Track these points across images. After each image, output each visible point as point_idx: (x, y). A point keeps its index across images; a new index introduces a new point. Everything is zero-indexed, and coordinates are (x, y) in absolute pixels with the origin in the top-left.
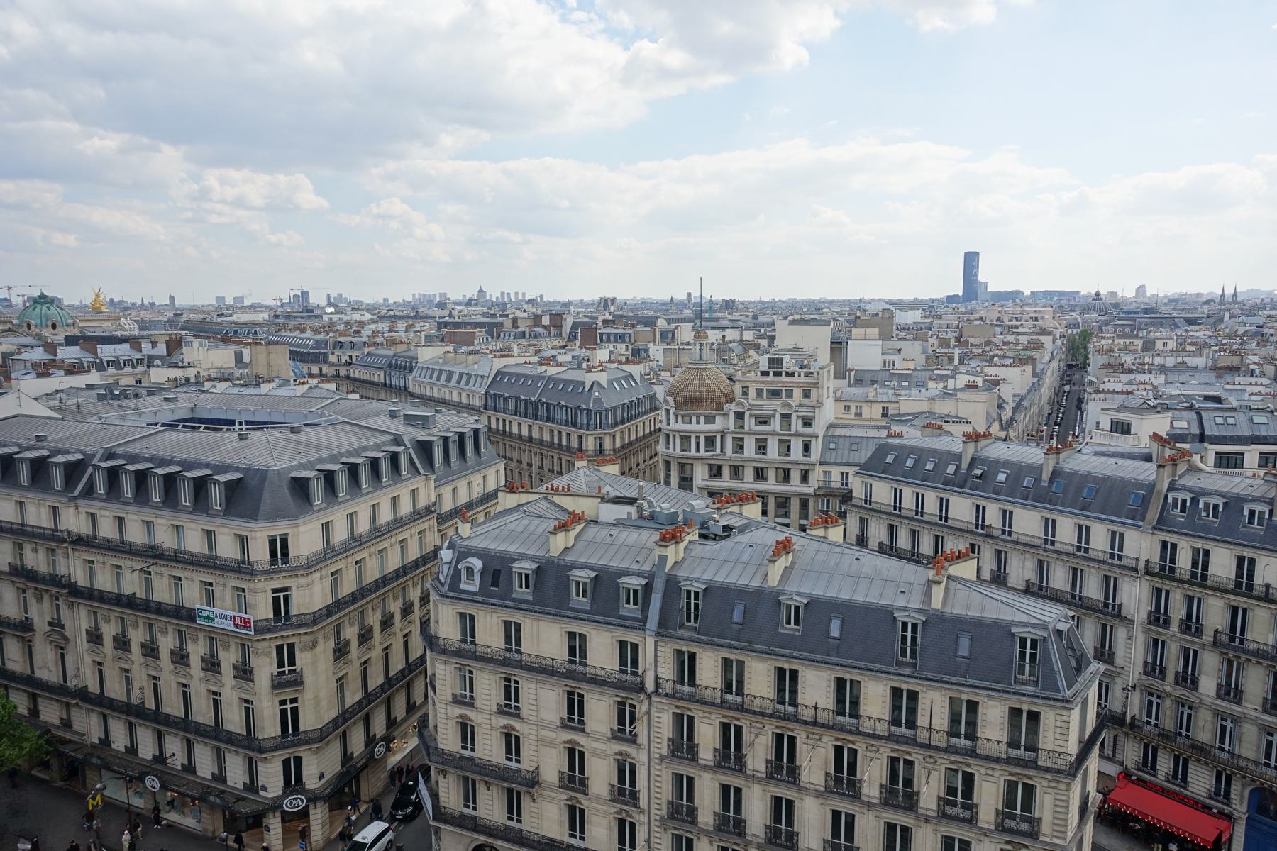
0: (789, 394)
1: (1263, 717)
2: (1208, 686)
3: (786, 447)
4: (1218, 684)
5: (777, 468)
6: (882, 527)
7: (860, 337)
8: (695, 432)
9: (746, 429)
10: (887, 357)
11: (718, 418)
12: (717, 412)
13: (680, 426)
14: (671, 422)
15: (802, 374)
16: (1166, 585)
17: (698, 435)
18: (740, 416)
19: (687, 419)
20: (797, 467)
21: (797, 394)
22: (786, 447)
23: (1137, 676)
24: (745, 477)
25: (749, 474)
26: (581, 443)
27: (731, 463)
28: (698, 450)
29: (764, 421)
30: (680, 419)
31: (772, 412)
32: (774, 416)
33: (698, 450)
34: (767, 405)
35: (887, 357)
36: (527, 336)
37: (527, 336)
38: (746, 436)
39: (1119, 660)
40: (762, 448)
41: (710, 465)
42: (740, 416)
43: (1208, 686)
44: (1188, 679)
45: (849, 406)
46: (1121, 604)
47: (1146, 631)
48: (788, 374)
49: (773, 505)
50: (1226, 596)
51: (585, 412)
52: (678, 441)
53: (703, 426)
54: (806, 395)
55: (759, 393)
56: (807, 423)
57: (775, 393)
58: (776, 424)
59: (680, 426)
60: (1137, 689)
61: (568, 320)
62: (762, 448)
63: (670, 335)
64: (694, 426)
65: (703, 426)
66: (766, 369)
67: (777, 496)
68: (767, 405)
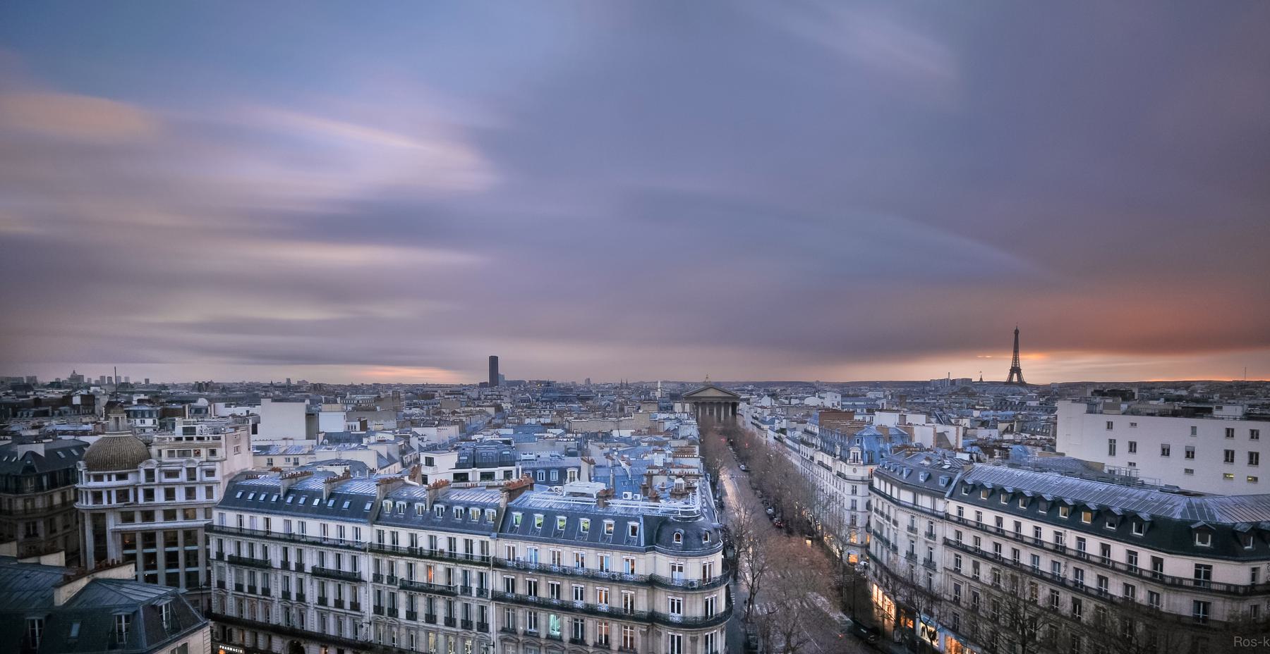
0: (198, 454)
1: (426, 625)
2: (402, 613)
3: (190, 493)
4: (407, 611)
5: (206, 508)
6: (232, 543)
7: (337, 410)
8: (106, 488)
9: (157, 481)
10: (350, 423)
11: (130, 476)
12: (129, 471)
13: (92, 484)
14: (84, 481)
15: (211, 439)
16: (380, 557)
17: (109, 490)
18: (150, 474)
19: (99, 478)
20: (201, 506)
21: (204, 452)
22: (190, 493)
23: (371, 615)
24: (197, 517)
25: (138, 517)
26: (10, 506)
27: (142, 509)
28: (110, 502)
29: (170, 474)
30: (92, 479)
31: (180, 468)
32: (181, 470)
33: (110, 502)
34: (177, 462)
35: (350, 423)
36: (50, 414)
37: (50, 414)
38: (156, 488)
39: (362, 608)
40: (170, 494)
41: (122, 512)
42: (150, 474)
43: (402, 613)
44: (393, 612)
45: (289, 459)
46: (360, 573)
47: (374, 586)
48: (199, 439)
49: (182, 537)
50: (405, 558)
51: (14, 478)
52: (90, 496)
53: (114, 482)
54: (213, 452)
55: (171, 453)
56: (211, 473)
57: (184, 454)
58: (183, 476)
59: (92, 484)
60: (372, 624)
61: (101, 400)
62: (170, 494)
63: (204, 411)
64: (105, 483)
65: (114, 482)
66: (181, 435)
67: (166, 532)
68: (177, 462)
